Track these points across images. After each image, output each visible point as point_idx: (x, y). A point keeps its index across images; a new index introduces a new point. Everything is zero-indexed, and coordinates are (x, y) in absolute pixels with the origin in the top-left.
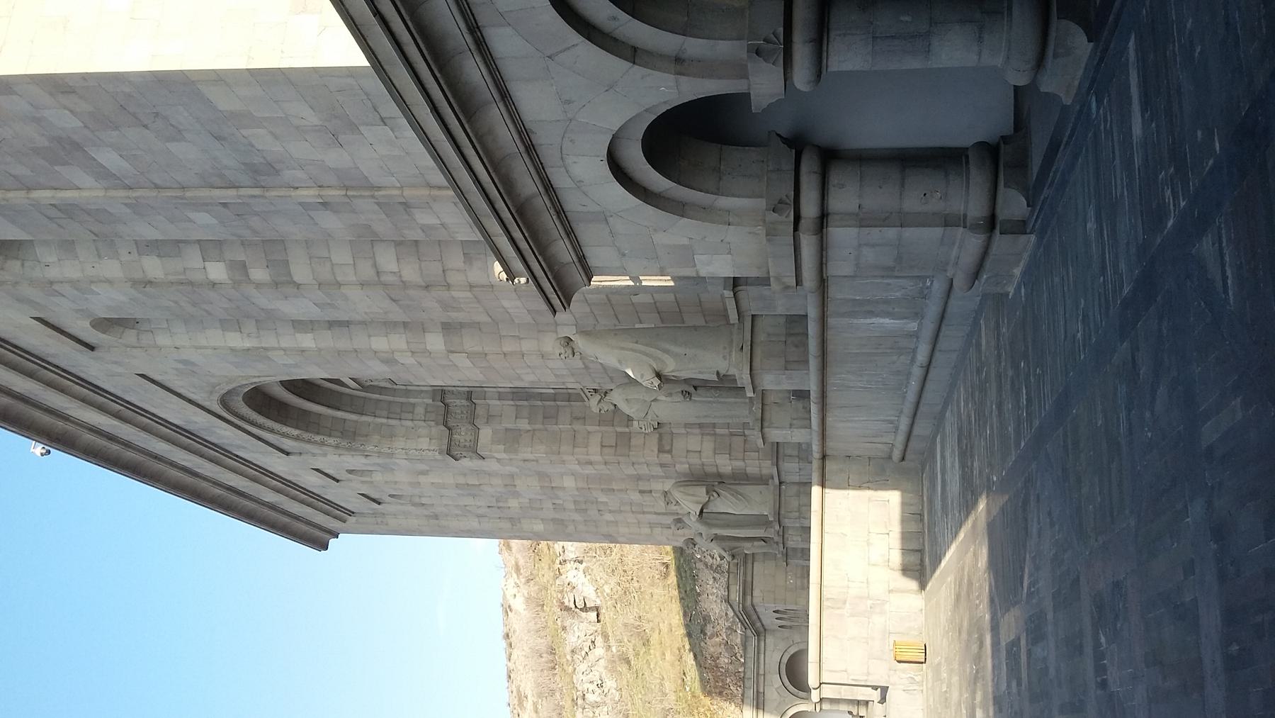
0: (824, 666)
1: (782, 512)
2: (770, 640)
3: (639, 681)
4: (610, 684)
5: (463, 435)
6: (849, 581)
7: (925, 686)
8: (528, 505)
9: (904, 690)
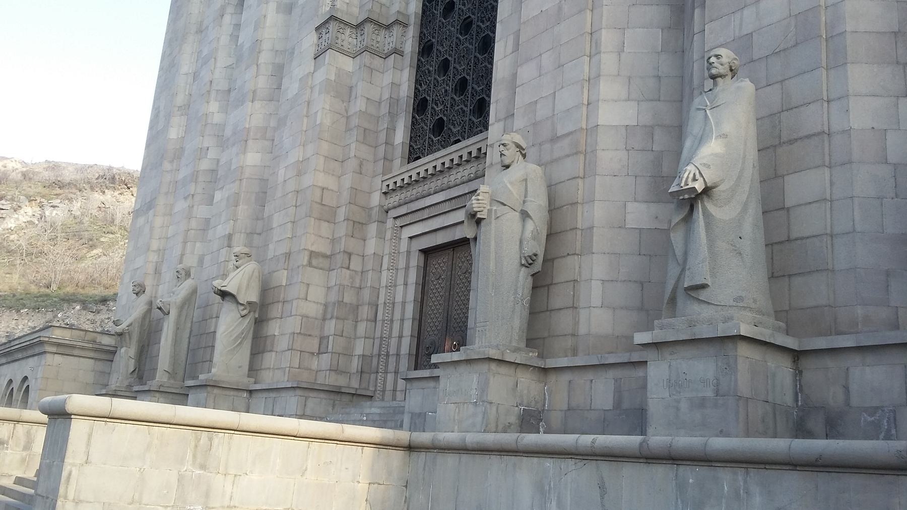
0: (100, 424)
1: (216, 391)
5: (348, 39)
6: (235, 476)
8: (209, 121)
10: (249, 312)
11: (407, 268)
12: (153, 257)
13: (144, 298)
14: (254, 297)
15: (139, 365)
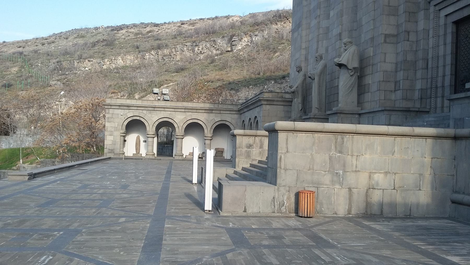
0: (290, 134)
1: (342, 115)
2: (236, 116)
3: (204, 67)
4: (202, 56)
6: (357, 156)
7: (278, 214)
9: (274, 198)
10: (355, 73)
11: (445, 35)
12: (303, 52)
13: (302, 73)
14: (356, 65)
15: (304, 107)
